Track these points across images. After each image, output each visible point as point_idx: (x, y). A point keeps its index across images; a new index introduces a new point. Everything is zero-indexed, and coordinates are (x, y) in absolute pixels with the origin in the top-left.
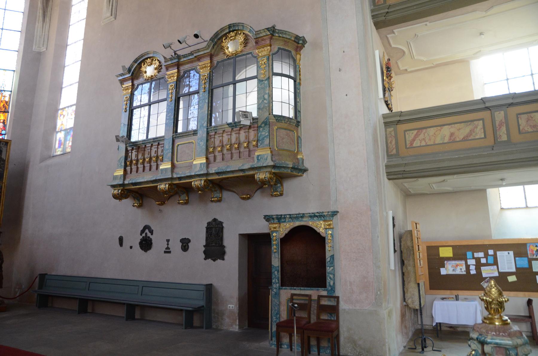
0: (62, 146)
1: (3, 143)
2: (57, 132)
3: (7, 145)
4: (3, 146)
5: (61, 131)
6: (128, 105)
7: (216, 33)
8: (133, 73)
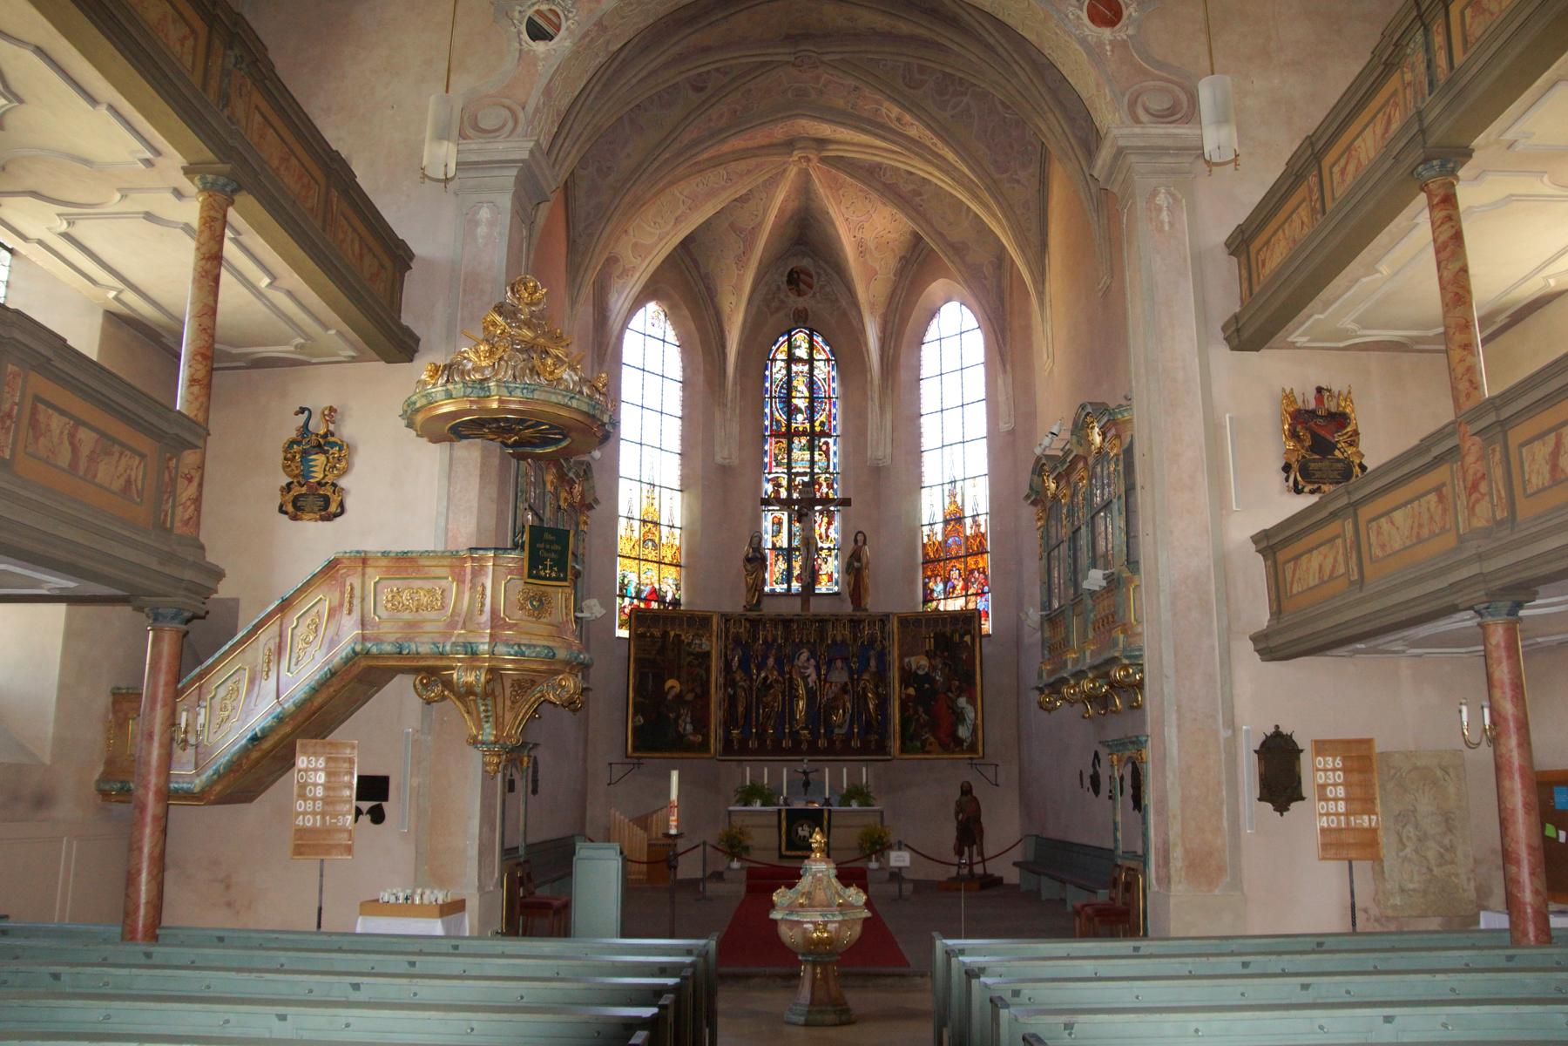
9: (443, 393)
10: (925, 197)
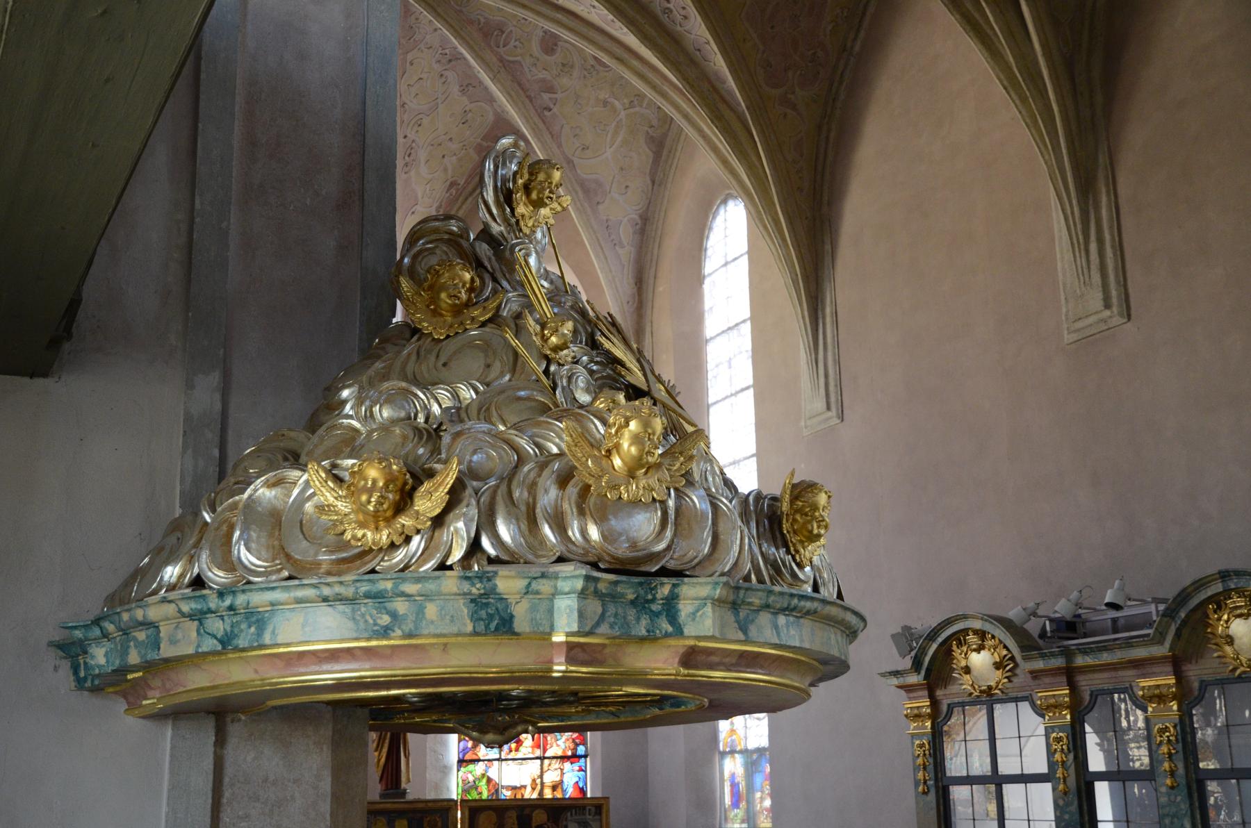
0: (743, 804)
1: (590, 810)
2: (723, 754)
3: (600, 814)
4: (591, 817)
5: (733, 752)
6: (930, 768)
7: (1179, 595)
8: (928, 670)
9: (463, 609)
10: (558, 96)
